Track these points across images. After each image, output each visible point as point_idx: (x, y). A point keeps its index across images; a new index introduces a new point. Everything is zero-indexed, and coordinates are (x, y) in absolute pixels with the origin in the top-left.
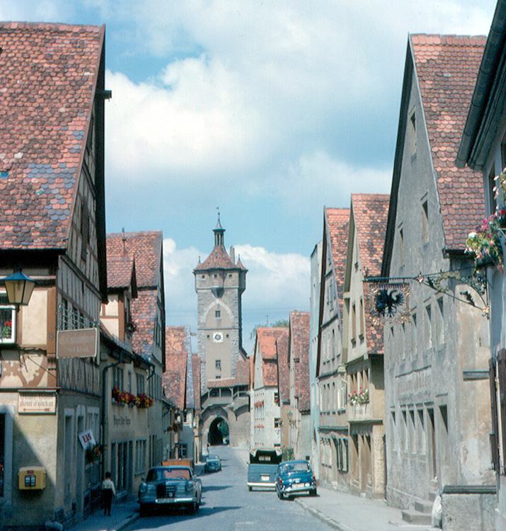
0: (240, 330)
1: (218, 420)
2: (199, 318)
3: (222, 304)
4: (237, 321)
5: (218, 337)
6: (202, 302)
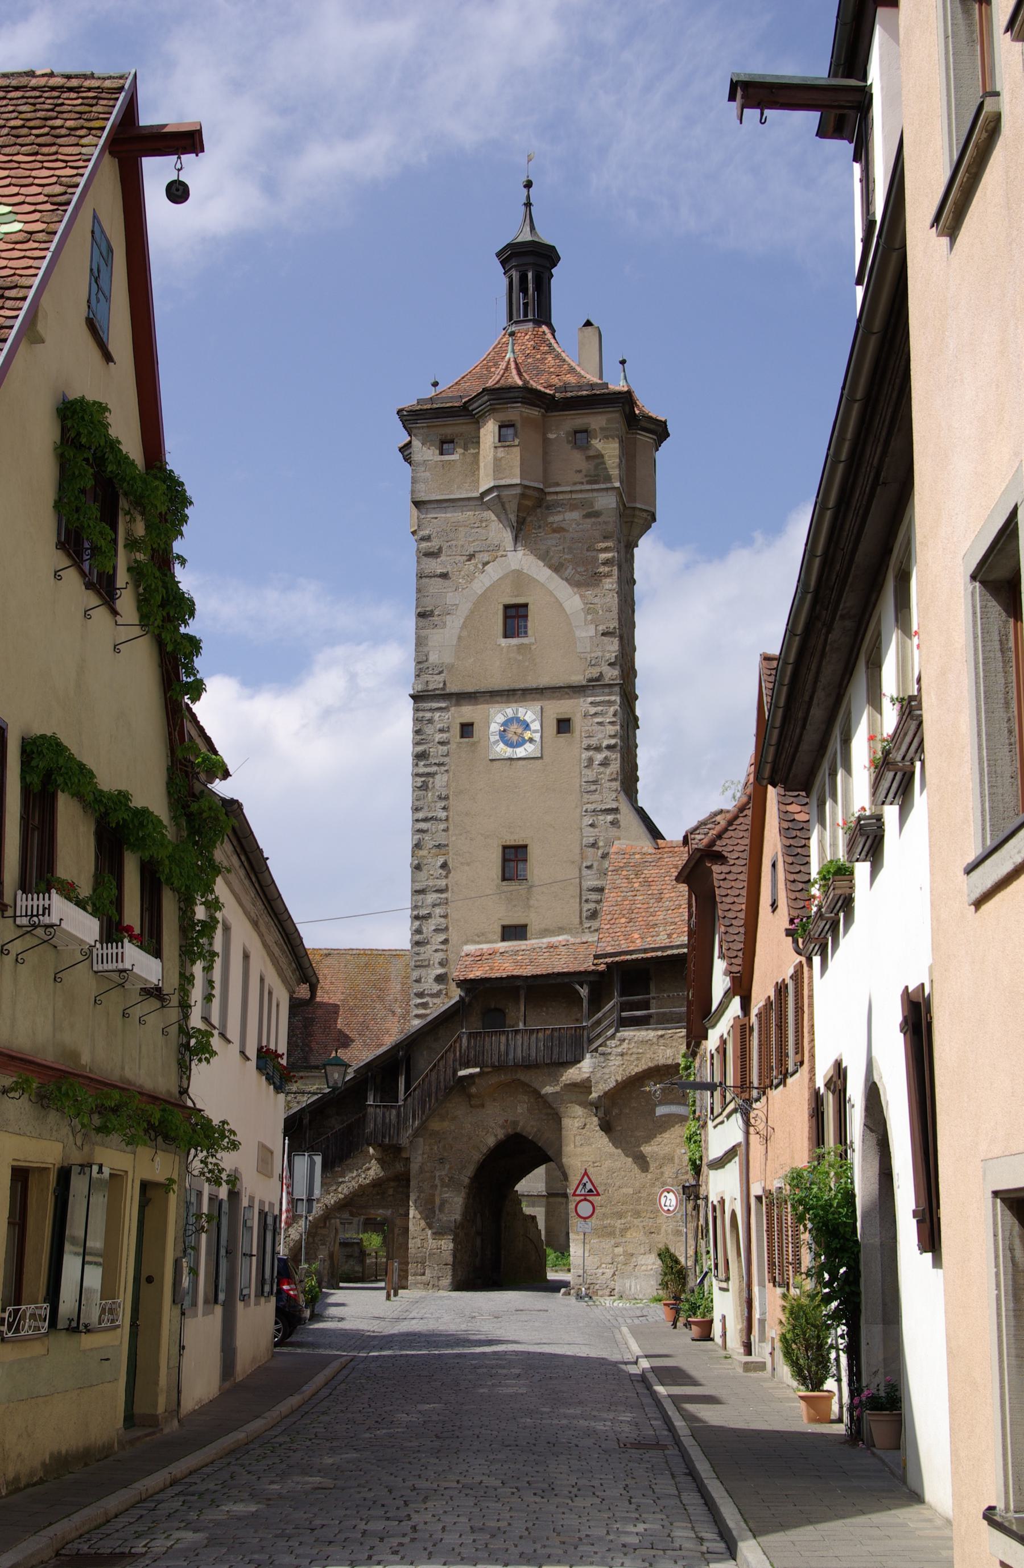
2: (420, 642)
4: (612, 647)
6: (435, 566)
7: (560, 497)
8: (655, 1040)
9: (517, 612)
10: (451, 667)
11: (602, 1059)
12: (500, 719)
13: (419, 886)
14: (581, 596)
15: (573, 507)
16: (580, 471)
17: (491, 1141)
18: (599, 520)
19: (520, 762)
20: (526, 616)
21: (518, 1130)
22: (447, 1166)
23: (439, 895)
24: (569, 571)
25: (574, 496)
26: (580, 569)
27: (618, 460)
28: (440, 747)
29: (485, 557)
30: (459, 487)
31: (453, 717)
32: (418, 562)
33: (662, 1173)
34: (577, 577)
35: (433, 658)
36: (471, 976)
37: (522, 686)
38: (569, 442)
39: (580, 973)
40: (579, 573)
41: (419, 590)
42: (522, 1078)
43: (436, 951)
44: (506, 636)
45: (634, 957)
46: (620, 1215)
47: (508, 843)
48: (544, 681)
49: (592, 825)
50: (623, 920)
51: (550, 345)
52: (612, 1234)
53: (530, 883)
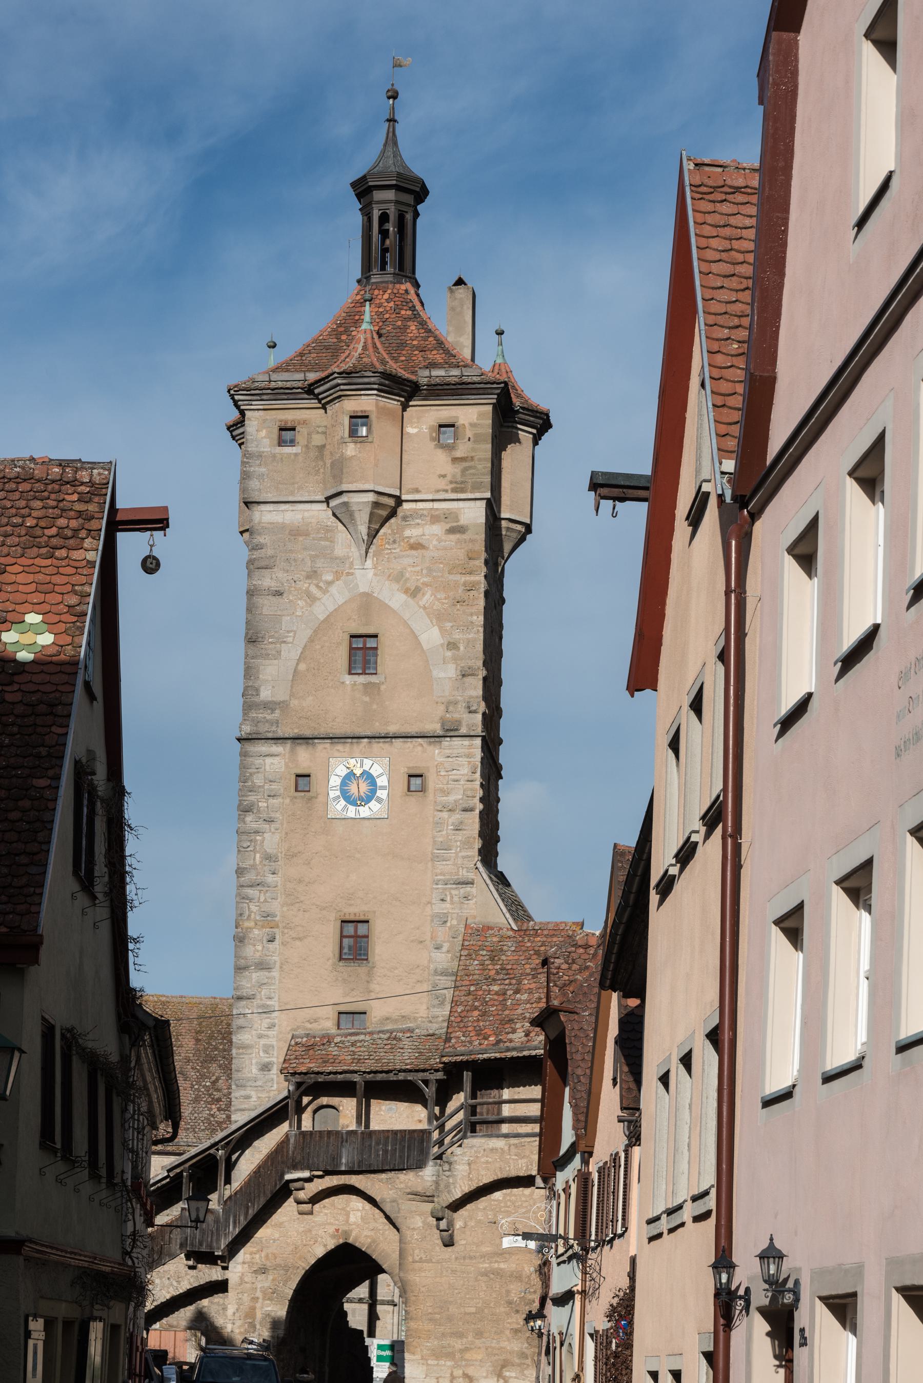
0: (491, 744)
1: (347, 1266)
2: (249, 672)
3: (396, 599)
4: (475, 688)
5: (360, 789)
7: (420, 505)
8: (506, 1148)
9: (365, 644)
10: (283, 706)
11: (446, 1167)
12: (342, 771)
13: (242, 962)
14: (440, 628)
15: (435, 519)
16: (444, 476)
17: (320, 1252)
18: (465, 537)
19: (366, 822)
20: (376, 649)
21: (350, 1241)
22: (271, 1277)
23: (267, 974)
24: (427, 598)
25: (437, 505)
26: (440, 595)
27: (489, 465)
28: (271, 801)
29: (329, 577)
30: (300, 488)
31: (287, 766)
32: (249, 575)
33: (508, 1292)
34: (437, 606)
35: (265, 694)
36: (303, 1069)
37: (369, 733)
38: (432, 439)
39: (424, 1071)
40: (438, 600)
41: (249, 610)
42: (357, 1185)
43: (260, 1036)
44: (350, 673)
45: (485, 1056)
46: (460, 1335)
47: (347, 918)
48: (392, 729)
49: (442, 900)
50: (476, 1013)
51: (413, 309)
52: (450, 1355)
53: (370, 964)
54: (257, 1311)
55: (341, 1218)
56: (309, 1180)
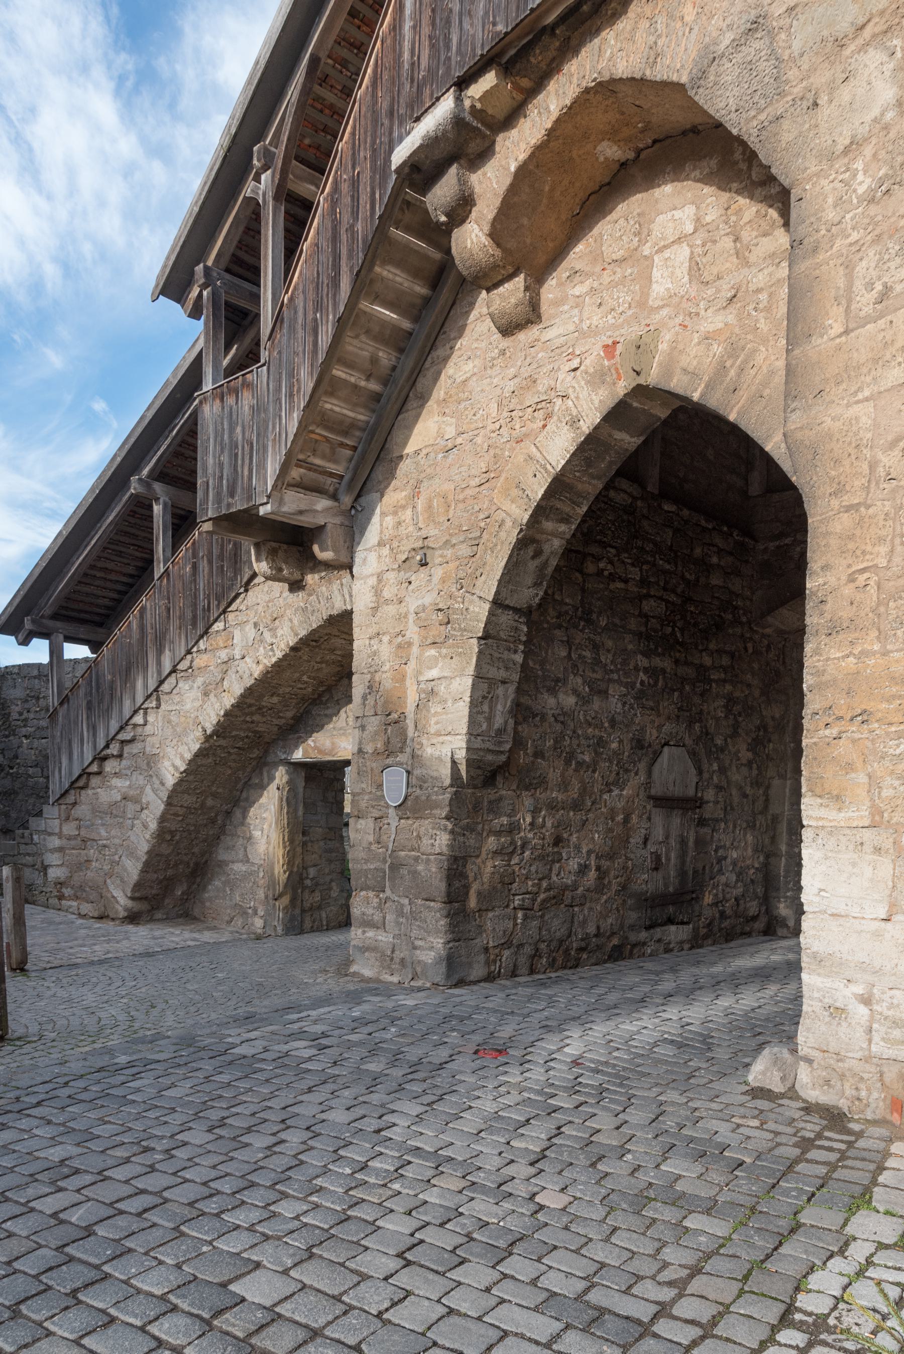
54: (408, 682)
55: (623, 297)
56: (467, 143)
